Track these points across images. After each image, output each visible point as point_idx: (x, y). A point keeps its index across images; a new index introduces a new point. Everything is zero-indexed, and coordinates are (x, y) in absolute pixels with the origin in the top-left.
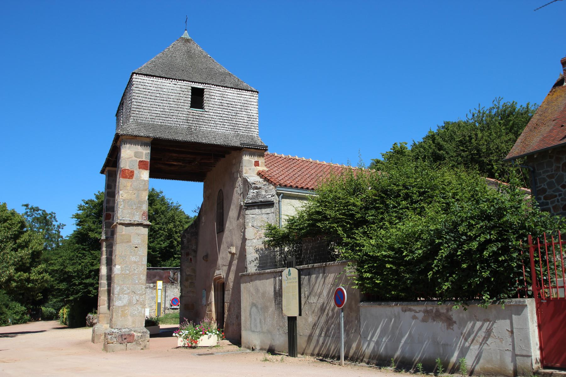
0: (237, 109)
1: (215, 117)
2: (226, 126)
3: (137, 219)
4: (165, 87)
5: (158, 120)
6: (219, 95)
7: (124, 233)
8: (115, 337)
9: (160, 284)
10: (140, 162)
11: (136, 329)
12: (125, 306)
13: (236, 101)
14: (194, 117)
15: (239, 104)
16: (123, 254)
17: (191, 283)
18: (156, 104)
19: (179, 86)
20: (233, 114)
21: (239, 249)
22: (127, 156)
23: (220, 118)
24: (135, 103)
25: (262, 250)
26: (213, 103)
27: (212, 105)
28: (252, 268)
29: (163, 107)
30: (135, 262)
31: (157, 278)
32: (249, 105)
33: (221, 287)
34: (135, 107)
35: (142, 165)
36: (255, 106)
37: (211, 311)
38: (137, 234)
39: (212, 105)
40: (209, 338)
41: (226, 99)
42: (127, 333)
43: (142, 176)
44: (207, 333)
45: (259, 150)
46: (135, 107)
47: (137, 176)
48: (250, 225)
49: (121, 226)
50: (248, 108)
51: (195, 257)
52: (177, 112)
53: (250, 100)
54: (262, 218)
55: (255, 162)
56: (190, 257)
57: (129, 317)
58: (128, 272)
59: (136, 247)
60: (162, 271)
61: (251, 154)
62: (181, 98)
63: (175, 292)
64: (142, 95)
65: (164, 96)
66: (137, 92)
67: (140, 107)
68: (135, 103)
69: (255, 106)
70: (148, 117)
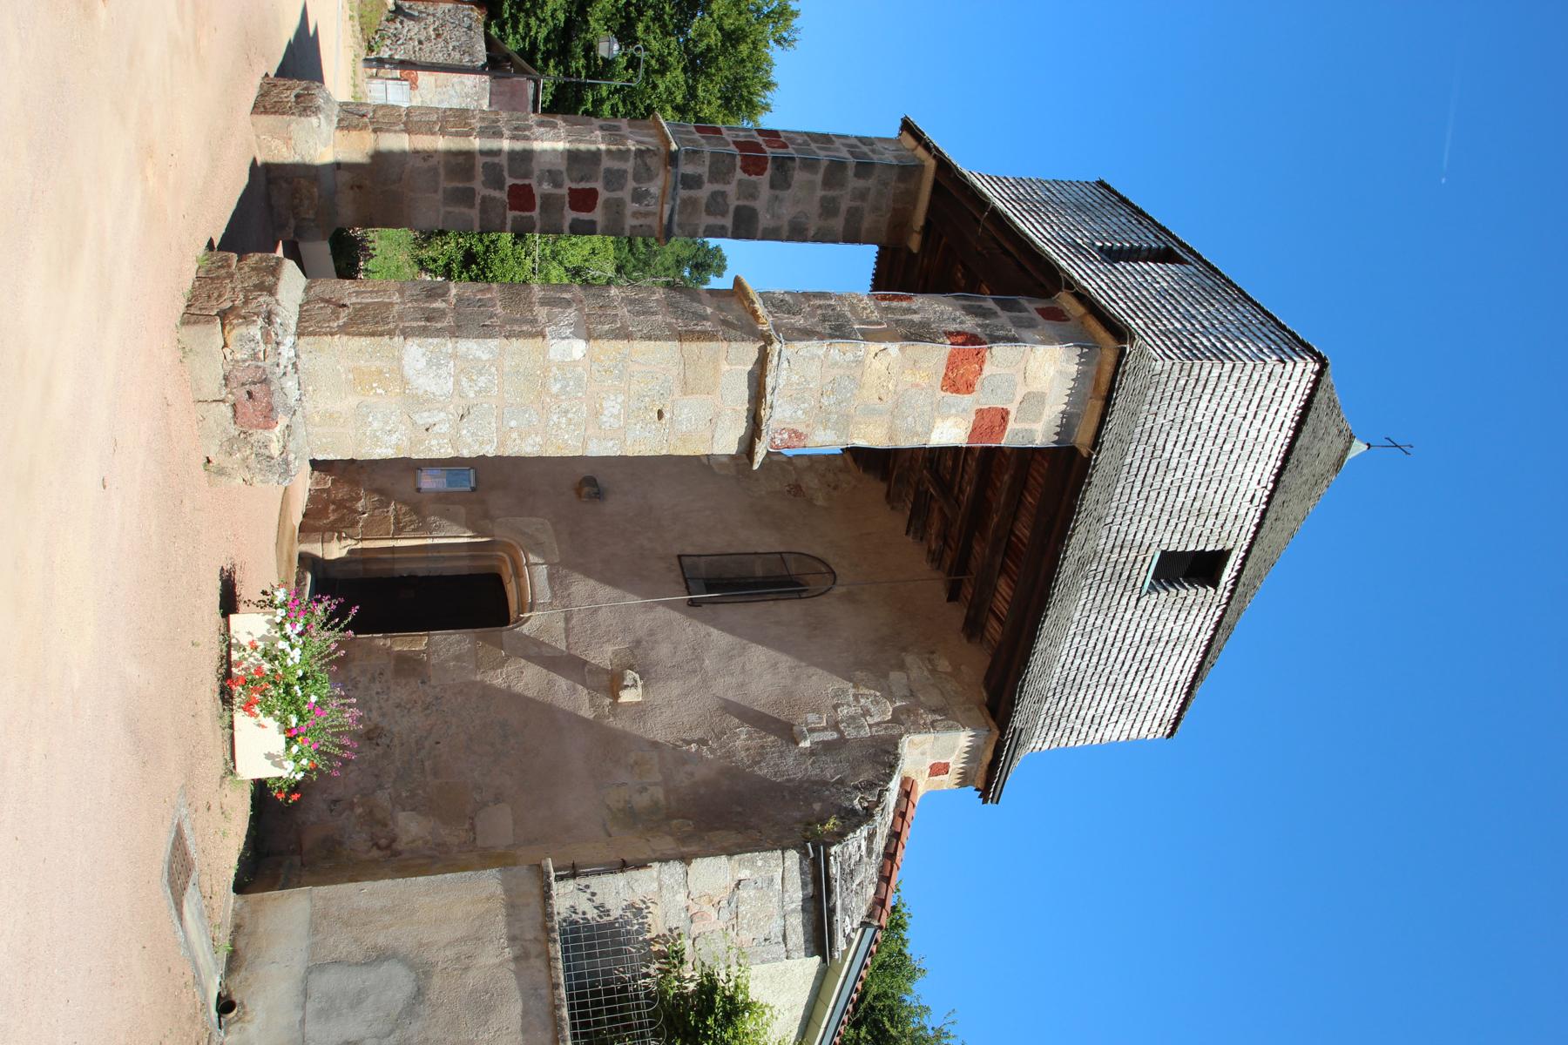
1: (1114, 628)
3: (778, 414)
5: (1139, 454)
6: (1185, 632)
7: (725, 367)
8: (255, 356)
10: (1004, 415)
12: (404, 382)
14: (1128, 566)
18: (1200, 442)
24: (1215, 373)
25: (644, 928)
27: (1155, 614)
28: (567, 898)
30: (597, 413)
32: (1132, 716)
34: (1204, 374)
37: (399, 531)
38: (718, 415)
40: (269, 756)
41: (1168, 652)
42: (277, 400)
43: (950, 422)
45: (987, 777)
46: (1204, 374)
48: (744, 874)
49: (754, 355)
53: (1150, 717)
54: (770, 917)
55: (946, 765)
57: (353, 401)
58: (555, 388)
59: (660, 414)
61: (973, 754)
64: (1239, 394)
65: (1220, 467)
66: (1256, 377)
67: (1198, 390)
68: (1215, 373)
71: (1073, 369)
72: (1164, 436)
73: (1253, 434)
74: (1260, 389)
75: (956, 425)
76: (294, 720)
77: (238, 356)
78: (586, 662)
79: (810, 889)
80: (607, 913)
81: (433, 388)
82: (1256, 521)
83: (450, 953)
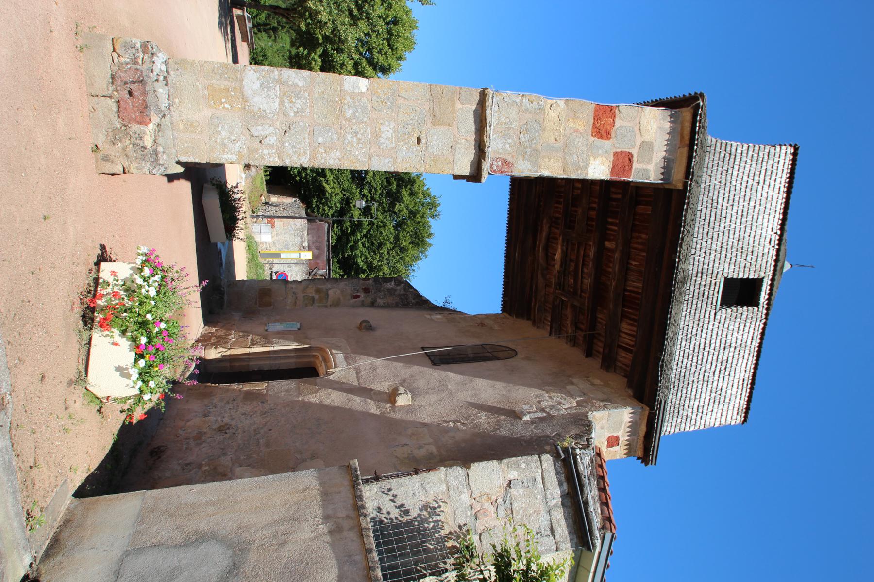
0: (715, 383)
1: (704, 336)
2: (685, 361)
4: (766, 220)
5: (705, 204)
7: (459, 106)
8: (135, 61)
9: (308, 255)
11: (169, 133)
12: (245, 100)
13: (731, 378)
15: (725, 386)
16: (401, 101)
17: (313, 299)
19: (766, 251)
20: (707, 374)
21: (410, 417)
22: (644, 121)
23: (702, 347)
25: (438, 526)
26: (731, 328)
27: (726, 326)
28: (373, 497)
29: (729, 216)
30: (377, 136)
31: (317, 252)
33: (305, 370)
35: (624, 160)
36: (718, 420)
37: (253, 344)
38: (456, 142)
39: (726, 326)
40: (119, 369)
42: (150, 99)
43: (599, 161)
44: (142, 363)
45: (646, 444)
47: (598, 148)
48: (513, 475)
49: (477, 98)
50: (716, 406)
51: (363, 305)
52: (719, 249)
54: (538, 513)
55: (617, 438)
56: (362, 295)
57: (207, 113)
58: (349, 113)
59: (419, 140)
60: (326, 258)
61: (634, 426)
62: (744, 255)
63: (296, 274)
65: (750, 218)
67: (731, 162)
69: (718, 420)
70: (713, 179)
71: (667, 125)
72: (716, 192)
73: (765, 195)
74: (764, 163)
75: (602, 163)
76: (144, 340)
77: (123, 60)
79: (565, 485)
80: (407, 512)
81: (264, 107)
82: (774, 257)
83: (268, 532)
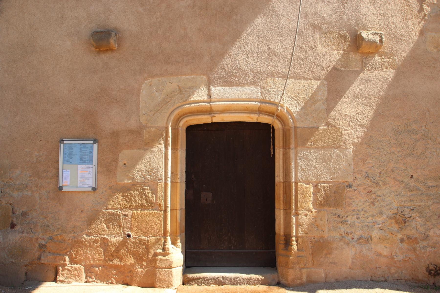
78: (334, 68)
